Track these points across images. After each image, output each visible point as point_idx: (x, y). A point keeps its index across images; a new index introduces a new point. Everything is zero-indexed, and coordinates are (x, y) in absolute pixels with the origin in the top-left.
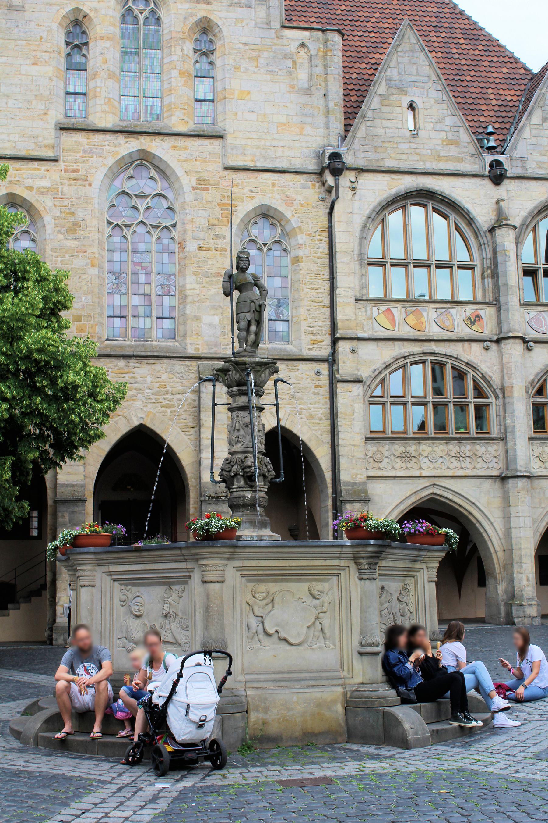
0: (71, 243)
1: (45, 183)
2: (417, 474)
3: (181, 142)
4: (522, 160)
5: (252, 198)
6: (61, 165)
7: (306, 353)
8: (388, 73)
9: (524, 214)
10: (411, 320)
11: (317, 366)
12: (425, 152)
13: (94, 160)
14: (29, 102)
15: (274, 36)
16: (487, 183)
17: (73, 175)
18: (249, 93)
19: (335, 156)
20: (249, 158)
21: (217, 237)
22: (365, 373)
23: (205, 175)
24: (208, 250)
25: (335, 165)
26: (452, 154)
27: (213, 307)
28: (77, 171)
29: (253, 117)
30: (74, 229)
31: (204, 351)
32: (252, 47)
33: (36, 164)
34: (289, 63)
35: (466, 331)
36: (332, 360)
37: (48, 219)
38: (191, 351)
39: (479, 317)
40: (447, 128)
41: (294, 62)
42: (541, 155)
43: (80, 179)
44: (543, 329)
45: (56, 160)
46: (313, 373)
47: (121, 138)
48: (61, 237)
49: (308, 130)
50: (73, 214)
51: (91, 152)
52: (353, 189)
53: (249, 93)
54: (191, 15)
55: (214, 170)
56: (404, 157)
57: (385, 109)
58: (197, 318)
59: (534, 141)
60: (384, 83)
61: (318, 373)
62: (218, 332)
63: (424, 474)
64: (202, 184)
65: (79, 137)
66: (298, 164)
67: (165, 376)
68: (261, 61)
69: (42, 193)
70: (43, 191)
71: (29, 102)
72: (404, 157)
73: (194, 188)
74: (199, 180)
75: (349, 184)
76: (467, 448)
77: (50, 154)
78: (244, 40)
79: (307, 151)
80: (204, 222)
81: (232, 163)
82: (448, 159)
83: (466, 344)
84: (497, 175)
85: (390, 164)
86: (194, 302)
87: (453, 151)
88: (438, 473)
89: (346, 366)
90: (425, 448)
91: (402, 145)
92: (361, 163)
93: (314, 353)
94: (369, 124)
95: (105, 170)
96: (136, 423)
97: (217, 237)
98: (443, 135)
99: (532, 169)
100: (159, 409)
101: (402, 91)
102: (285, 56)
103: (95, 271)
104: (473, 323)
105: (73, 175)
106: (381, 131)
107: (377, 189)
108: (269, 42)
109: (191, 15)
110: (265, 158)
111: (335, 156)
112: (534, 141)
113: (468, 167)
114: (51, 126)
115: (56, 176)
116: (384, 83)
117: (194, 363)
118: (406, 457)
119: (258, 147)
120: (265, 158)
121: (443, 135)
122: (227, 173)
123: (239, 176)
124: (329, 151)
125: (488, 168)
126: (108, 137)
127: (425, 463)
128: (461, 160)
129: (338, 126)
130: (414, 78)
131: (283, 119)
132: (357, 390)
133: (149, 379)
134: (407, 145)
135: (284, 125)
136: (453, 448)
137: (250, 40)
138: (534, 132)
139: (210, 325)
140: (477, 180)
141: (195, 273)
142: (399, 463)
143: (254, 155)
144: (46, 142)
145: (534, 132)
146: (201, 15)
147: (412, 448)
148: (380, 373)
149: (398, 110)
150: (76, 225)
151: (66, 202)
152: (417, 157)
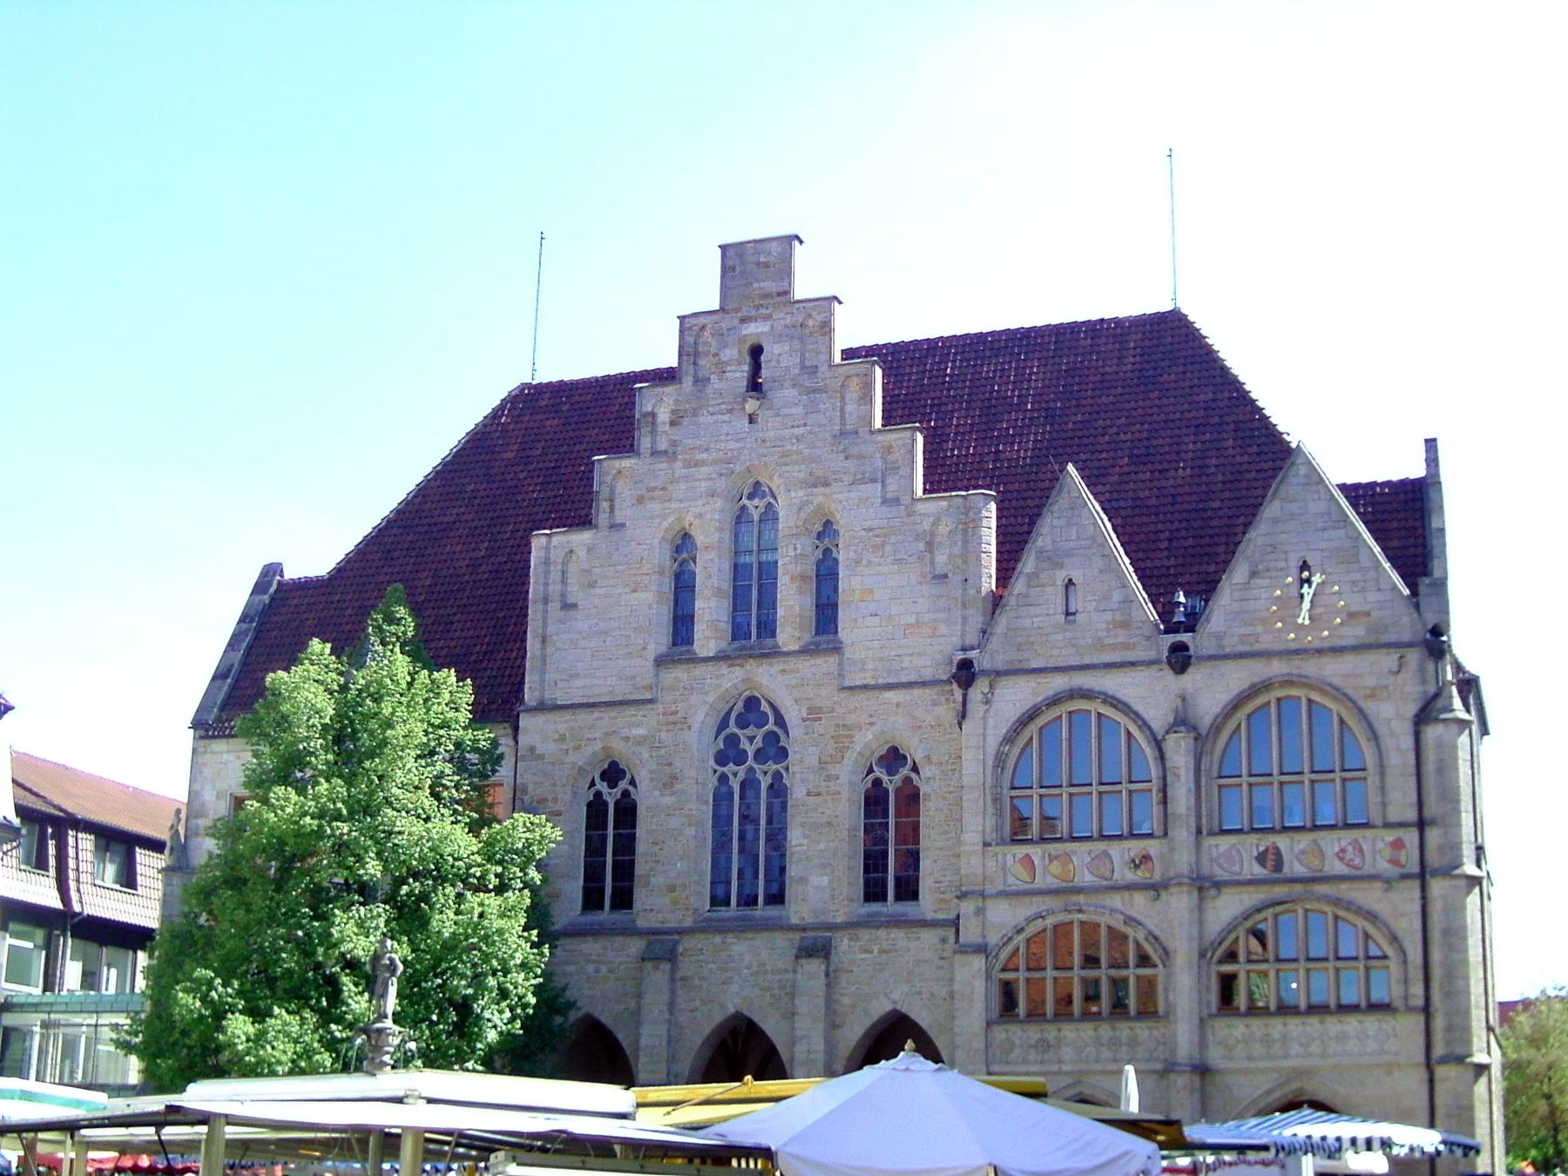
0: (668, 800)
1: (641, 731)
2: (1055, 1068)
3: (791, 664)
4: (1219, 637)
5: (872, 724)
6: (660, 708)
7: (930, 916)
8: (1039, 543)
9: (1217, 710)
10: (1055, 867)
11: (940, 932)
12: (1082, 642)
13: (694, 699)
14: (628, 637)
15: (903, 514)
16: (1168, 673)
17: (671, 719)
18: (872, 591)
19: (966, 665)
20: (870, 674)
21: (829, 778)
22: (993, 939)
23: (818, 703)
24: (819, 794)
25: (965, 674)
26: (1120, 640)
27: (823, 866)
28: (674, 713)
29: (876, 620)
30: (670, 783)
31: (810, 920)
32: (877, 532)
33: (632, 710)
34: (921, 546)
35: (1131, 876)
36: (955, 923)
37: (643, 777)
38: (794, 920)
39: (1146, 858)
40: (1113, 606)
41: (930, 547)
42: (1247, 624)
43: (679, 722)
44: (1237, 868)
45: (650, 701)
46: (937, 940)
47: (723, 668)
48: (657, 793)
49: (943, 629)
50: (670, 764)
51: (692, 688)
52: (987, 702)
53: (872, 591)
54: (807, 503)
55: (827, 695)
56: (1056, 652)
57: (1034, 592)
58: (803, 880)
59: (1236, 606)
60: (1033, 556)
61: (944, 941)
62: (827, 897)
63: (1065, 1068)
64: (814, 714)
65: (679, 674)
66: (928, 674)
67: (764, 954)
68: (888, 548)
69: (639, 743)
70: (640, 741)
71: (628, 637)
72: (1056, 652)
73: (804, 720)
74: (810, 710)
75: (980, 697)
76: (1124, 1029)
77: (648, 696)
78: (867, 524)
79: (939, 657)
80: (814, 761)
81: (847, 683)
82: (1115, 647)
83: (1126, 894)
84: (1180, 659)
85: (1034, 665)
86: (799, 861)
87: (1121, 636)
88: (1083, 1066)
89: (970, 933)
90: (1069, 1031)
91: (1053, 637)
92: (1000, 666)
93: (940, 916)
94: (1012, 614)
95: (705, 709)
96: (732, 1010)
97: (829, 778)
98: (1108, 616)
99: (1231, 645)
100: (757, 991)
101: (1059, 565)
102: (918, 537)
103: (691, 831)
104: (1137, 867)
105: (671, 719)
106: (1027, 622)
107: (1015, 697)
108: (897, 522)
109: (807, 503)
110: (889, 672)
111: (966, 665)
112: (1236, 606)
113: (1139, 654)
114: (650, 664)
115: (654, 723)
116: (1033, 556)
117: (798, 936)
118: (1044, 1045)
119: (881, 659)
120: (889, 672)
121: (1108, 616)
122: (844, 695)
123: (861, 698)
124: (960, 656)
125: (1166, 654)
126: (710, 666)
127: (1067, 1053)
128: (1127, 647)
129: (976, 620)
130: (1072, 544)
131: (912, 620)
132: (978, 962)
133: (747, 958)
134: (1060, 637)
135: (912, 625)
136: (1105, 1030)
137: (875, 523)
138: (1237, 594)
139: (819, 888)
140: (1153, 670)
141: (802, 825)
142: (1032, 1055)
143: (875, 670)
144: (644, 683)
145: (1237, 594)
146: (819, 500)
147: (1051, 1032)
148: (1010, 939)
149: (1049, 589)
150: (674, 778)
151: (663, 752)
152: (1073, 650)
